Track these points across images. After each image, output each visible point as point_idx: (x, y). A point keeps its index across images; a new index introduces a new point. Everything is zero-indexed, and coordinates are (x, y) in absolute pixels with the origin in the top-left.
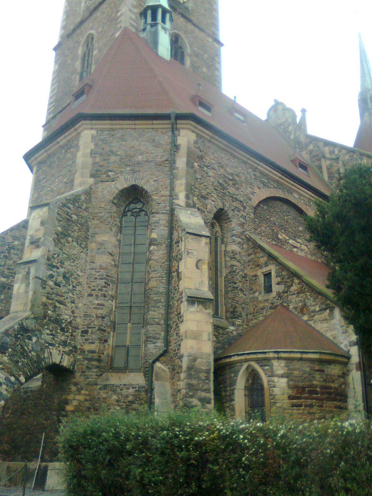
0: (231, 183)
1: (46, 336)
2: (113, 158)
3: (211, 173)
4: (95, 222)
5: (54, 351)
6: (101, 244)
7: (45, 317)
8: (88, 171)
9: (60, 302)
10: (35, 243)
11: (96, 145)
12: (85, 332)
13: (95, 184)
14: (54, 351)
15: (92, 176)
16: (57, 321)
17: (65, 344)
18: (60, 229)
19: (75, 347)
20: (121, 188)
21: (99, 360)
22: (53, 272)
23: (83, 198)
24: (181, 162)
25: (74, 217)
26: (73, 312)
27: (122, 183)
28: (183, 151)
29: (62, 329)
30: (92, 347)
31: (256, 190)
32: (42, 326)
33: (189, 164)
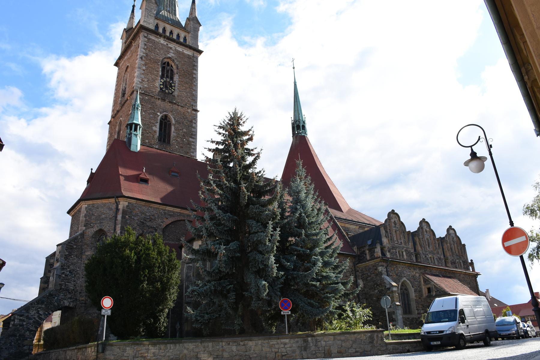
0: (148, 220)
1: (61, 296)
2: (93, 217)
3: (136, 219)
4: (86, 246)
5: (66, 301)
6: (87, 256)
7: (61, 289)
8: (83, 224)
12: (80, 293)
13: (86, 229)
14: (66, 301)
15: (84, 226)
16: (67, 290)
17: (71, 298)
18: (67, 253)
19: (76, 299)
21: (85, 304)
22: (65, 271)
23: (79, 237)
24: (119, 217)
26: (75, 285)
27: (96, 229)
29: (69, 293)
30: (83, 299)
31: (165, 220)
32: (60, 292)
33: (123, 217)
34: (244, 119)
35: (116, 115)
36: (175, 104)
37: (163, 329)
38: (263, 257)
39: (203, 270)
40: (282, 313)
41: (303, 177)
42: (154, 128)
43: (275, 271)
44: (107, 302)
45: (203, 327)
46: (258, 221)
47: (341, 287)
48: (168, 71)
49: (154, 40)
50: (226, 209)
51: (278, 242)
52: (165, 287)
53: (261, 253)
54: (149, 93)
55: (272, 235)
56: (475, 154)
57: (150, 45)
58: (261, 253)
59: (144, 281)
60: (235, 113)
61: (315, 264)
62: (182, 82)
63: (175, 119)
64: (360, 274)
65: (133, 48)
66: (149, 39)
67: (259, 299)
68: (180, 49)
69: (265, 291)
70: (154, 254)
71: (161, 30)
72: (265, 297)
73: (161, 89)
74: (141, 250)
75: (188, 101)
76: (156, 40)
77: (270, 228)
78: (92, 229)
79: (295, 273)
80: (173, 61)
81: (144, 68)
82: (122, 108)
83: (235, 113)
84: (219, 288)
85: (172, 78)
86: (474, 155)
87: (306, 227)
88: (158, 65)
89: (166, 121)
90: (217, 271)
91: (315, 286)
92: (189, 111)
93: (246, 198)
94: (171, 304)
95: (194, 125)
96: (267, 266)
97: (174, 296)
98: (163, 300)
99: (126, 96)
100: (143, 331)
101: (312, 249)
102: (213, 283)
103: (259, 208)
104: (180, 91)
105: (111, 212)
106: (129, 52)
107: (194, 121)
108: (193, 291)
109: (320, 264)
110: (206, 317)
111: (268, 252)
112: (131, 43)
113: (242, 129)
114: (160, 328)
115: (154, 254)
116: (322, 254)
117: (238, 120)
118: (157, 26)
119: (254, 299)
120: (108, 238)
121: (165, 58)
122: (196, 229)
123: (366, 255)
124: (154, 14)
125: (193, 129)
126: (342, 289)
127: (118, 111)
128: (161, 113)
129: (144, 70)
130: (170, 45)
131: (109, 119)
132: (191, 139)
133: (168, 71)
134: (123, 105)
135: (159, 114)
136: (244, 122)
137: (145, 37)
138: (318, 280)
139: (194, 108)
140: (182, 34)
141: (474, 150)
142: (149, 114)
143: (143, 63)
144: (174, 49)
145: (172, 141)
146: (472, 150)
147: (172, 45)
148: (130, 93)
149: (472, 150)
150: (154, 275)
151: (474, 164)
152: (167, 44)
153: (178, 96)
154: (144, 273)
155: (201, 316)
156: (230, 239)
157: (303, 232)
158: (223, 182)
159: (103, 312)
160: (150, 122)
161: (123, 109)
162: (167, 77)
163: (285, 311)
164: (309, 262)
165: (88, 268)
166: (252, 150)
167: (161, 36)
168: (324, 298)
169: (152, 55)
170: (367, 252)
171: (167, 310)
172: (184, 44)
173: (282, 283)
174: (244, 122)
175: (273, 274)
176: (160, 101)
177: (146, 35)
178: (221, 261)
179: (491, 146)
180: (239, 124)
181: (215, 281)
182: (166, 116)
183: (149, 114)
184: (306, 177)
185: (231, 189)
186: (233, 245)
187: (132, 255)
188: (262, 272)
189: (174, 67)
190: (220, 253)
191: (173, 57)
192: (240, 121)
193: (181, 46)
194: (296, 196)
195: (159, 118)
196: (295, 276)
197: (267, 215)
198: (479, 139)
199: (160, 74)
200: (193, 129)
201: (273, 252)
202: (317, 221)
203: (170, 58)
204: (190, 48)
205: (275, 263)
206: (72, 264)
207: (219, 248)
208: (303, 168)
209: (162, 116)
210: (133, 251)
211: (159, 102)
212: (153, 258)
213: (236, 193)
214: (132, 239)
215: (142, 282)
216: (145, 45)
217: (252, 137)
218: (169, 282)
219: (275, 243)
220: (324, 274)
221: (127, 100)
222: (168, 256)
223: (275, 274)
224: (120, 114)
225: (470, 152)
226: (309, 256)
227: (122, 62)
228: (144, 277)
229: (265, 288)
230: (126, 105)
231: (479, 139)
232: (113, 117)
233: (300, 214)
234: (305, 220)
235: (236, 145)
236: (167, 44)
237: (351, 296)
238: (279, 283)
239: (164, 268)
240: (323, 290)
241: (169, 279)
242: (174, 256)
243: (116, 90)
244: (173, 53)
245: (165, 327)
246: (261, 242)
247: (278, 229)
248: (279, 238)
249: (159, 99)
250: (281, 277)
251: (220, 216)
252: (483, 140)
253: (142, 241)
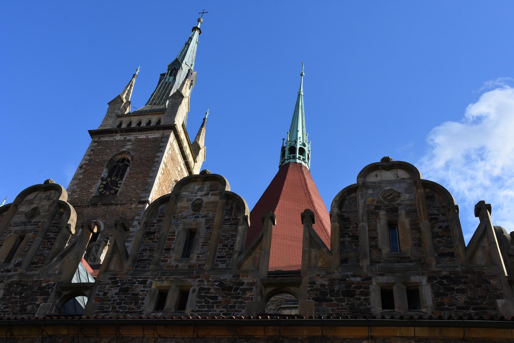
36: (112, 204)
49: (107, 141)
54: (77, 204)
57: (99, 148)
62: (133, 173)
63: (105, 224)
66: (101, 141)
68: (142, 136)
80: (129, 153)
104: (126, 186)
129: (80, 179)
130: (128, 138)
143: (83, 171)
147: (132, 137)
152: (125, 138)
162: (116, 176)
176: (89, 209)
193: (145, 132)
203: (124, 152)
244: (131, 145)
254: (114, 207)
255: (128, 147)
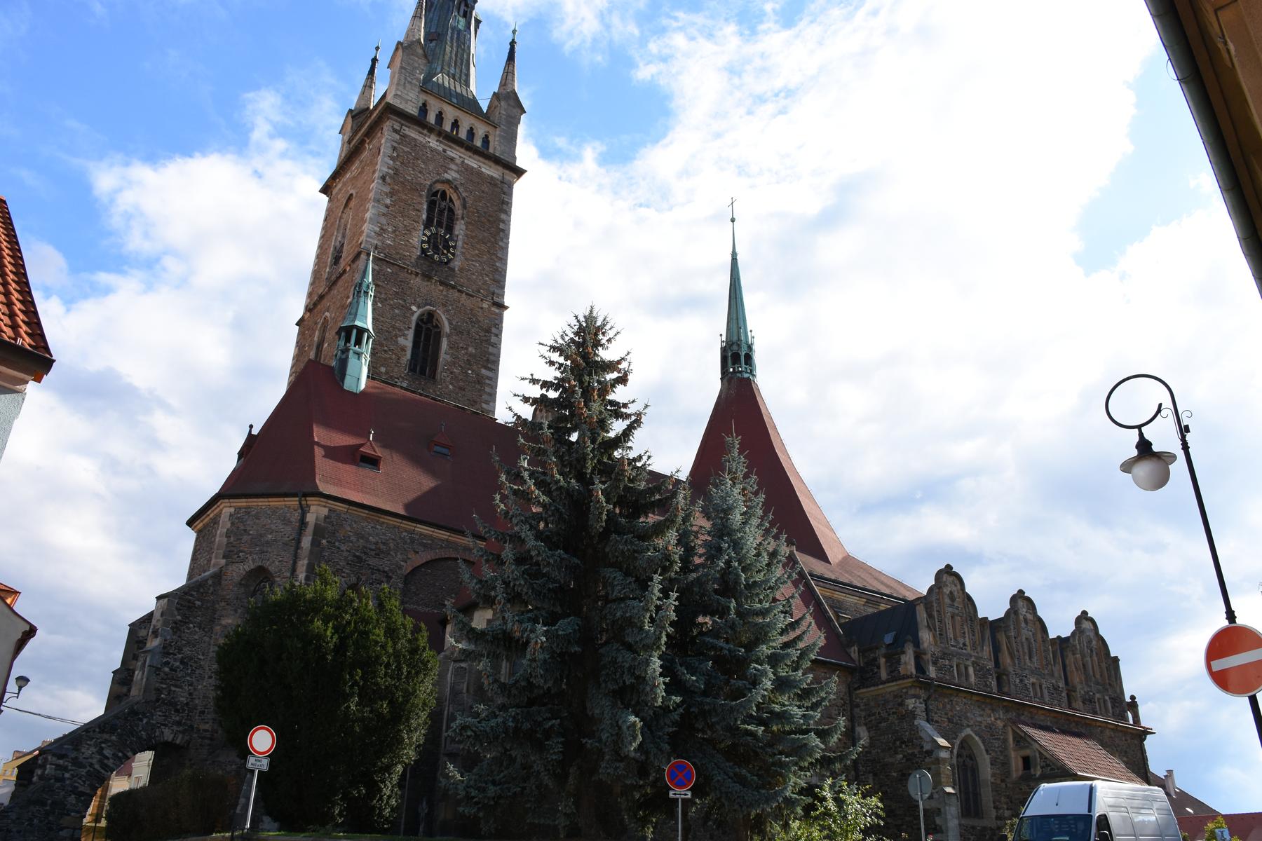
1: (158, 716)
2: (245, 538)
3: (343, 548)
4: (223, 604)
7: (158, 700)
9: (176, 686)
10: (155, 634)
11: (232, 524)
12: (202, 712)
13: (227, 565)
15: (224, 557)
16: (172, 704)
17: (179, 723)
18: (179, 618)
19: (191, 727)
20: (247, 569)
21: (211, 739)
23: (210, 582)
24: (306, 542)
25: (198, 603)
26: (191, 694)
27: (249, 565)
28: (310, 529)
29: (177, 711)
30: (207, 727)
31: (411, 555)
33: (315, 543)
34: (611, 334)
35: (315, 305)
36: (453, 287)
37: (387, 812)
38: (634, 659)
39: (491, 679)
40: (671, 795)
41: (740, 475)
42: (401, 340)
43: (661, 692)
44: (262, 740)
45: (481, 814)
46: (627, 574)
47: (814, 740)
48: (441, 212)
50: (555, 539)
51: (672, 624)
52: (400, 714)
53: (630, 648)
55: (658, 608)
56: (1149, 444)
58: (630, 648)
59: (352, 695)
60: (590, 318)
61: (755, 682)
63: (450, 323)
64: (863, 714)
65: (365, 155)
66: (405, 136)
67: (619, 756)
68: (473, 162)
69: (635, 738)
70: (379, 633)
71: (431, 118)
72: (632, 755)
73: (423, 251)
74: (349, 623)
75: (485, 283)
76: (420, 138)
77: (656, 591)
78: (241, 566)
79: (708, 700)
80: (456, 189)
81: (388, 201)
82: (330, 289)
83: (590, 318)
84: (526, 726)
85: (450, 229)
86: (1144, 447)
87: (741, 592)
88: (421, 196)
89: (429, 326)
90: (523, 684)
91: (753, 734)
92: (485, 305)
93: (604, 517)
94: (410, 754)
95: (493, 339)
96: (641, 680)
97: (418, 736)
98: (396, 743)
99: (342, 263)
100: (340, 815)
101: (751, 646)
102: (512, 711)
103: (632, 543)
105: (289, 528)
106: (357, 164)
107: (494, 330)
108: (464, 728)
109: (769, 685)
110: (492, 790)
111: (649, 648)
112: (362, 142)
113: (605, 354)
114: (381, 810)
115: (379, 633)
116: (774, 660)
117: (596, 335)
118: (424, 109)
119: (607, 757)
120: (277, 589)
121: (437, 181)
122: (481, 581)
123: (879, 667)
124: (418, 80)
125: (491, 349)
126: (817, 746)
127: (321, 297)
128: (419, 307)
129: (387, 207)
130: (450, 153)
131: (299, 312)
132: (484, 371)
133: (441, 212)
134: (335, 283)
135: (414, 308)
136: (609, 340)
137: (395, 131)
138: (761, 722)
139: (496, 299)
140: (481, 130)
141: (1147, 436)
142: (392, 307)
143: (387, 189)
144: (458, 161)
145: (442, 373)
146: (1141, 435)
147: (455, 153)
148: (351, 257)
149: (1141, 435)
150: (377, 684)
151: (1144, 469)
152: (444, 151)
153: (461, 270)
154: (352, 676)
155: (479, 789)
156: (558, 609)
157: (733, 604)
158: (553, 476)
159: (251, 760)
160: (394, 327)
161: (335, 292)
162: (440, 224)
163: (678, 791)
164: (743, 677)
165: (224, 655)
166: (625, 405)
167: (431, 130)
168: (774, 764)
169: (409, 174)
170: (882, 661)
171: (399, 768)
172: (483, 153)
173: (674, 723)
174: (609, 340)
175: (655, 699)
177: (397, 127)
178: (534, 660)
179: (1187, 429)
180: (597, 344)
181: (517, 706)
182: (431, 315)
183: (392, 307)
184: (746, 476)
185: (569, 493)
186: (565, 626)
187: (329, 633)
188: (631, 693)
189: (457, 203)
190: (532, 644)
191: (455, 179)
192: (601, 337)
194: (722, 519)
195: (415, 318)
196: (707, 708)
197: (650, 560)
198: (1159, 411)
199: (424, 217)
200: (491, 349)
201: (658, 648)
202: (768, 581)
203: (448, 182)
204: (497, 161)
205: (661, 675)
206: (189, 643)
207: (533, 631)
208: (740, 453)
209: (422, 315)
210: (331, 625)
211: (416, 282)
212: (377, 642)
213: (580, 504)
214: (332, 594)
215: (346, 698)
216: (394, 149)
217: (626, 375)
218: (407, 701)
219: (664, 628)
220: (777, 708)
221: (345, 271)
222: (409, 641)
223: (660, 700)
224: (326, 302)
225: (1137, 439)
226: (743, 663)
227: (340, 186)
228: (352, 687)
229: (634, 731)
230: (340, 283)
231: (1159, 411)
232: (309, 309)
233: (728, 563)
234: (738, 576)
235: (587, 392)
236: (444, 151)
237: (838, 765)
238: (668, 721)
239: (399, 668)
240: (771, 744)
241: (408, 695)
242: (423, 642)
243: (320, 247)
245: (393, 810)
246: (631, 623)
247: (674, 595)
248: (673, 616)
249: (417, 274)
250: (675, 709)
251: (539, 554)
252: (1168, 412)
253: (352, 601)
254: (457, 294)
255: (455, 175)
